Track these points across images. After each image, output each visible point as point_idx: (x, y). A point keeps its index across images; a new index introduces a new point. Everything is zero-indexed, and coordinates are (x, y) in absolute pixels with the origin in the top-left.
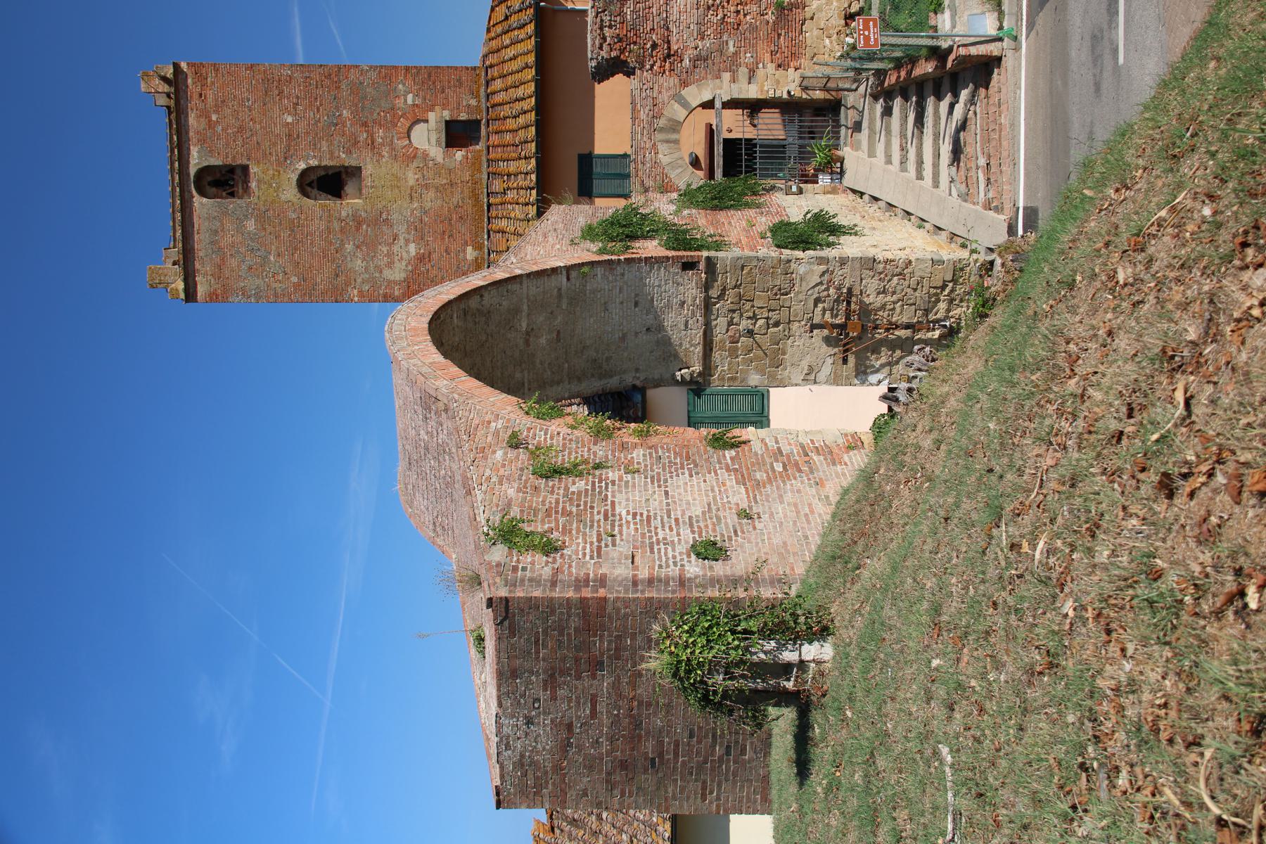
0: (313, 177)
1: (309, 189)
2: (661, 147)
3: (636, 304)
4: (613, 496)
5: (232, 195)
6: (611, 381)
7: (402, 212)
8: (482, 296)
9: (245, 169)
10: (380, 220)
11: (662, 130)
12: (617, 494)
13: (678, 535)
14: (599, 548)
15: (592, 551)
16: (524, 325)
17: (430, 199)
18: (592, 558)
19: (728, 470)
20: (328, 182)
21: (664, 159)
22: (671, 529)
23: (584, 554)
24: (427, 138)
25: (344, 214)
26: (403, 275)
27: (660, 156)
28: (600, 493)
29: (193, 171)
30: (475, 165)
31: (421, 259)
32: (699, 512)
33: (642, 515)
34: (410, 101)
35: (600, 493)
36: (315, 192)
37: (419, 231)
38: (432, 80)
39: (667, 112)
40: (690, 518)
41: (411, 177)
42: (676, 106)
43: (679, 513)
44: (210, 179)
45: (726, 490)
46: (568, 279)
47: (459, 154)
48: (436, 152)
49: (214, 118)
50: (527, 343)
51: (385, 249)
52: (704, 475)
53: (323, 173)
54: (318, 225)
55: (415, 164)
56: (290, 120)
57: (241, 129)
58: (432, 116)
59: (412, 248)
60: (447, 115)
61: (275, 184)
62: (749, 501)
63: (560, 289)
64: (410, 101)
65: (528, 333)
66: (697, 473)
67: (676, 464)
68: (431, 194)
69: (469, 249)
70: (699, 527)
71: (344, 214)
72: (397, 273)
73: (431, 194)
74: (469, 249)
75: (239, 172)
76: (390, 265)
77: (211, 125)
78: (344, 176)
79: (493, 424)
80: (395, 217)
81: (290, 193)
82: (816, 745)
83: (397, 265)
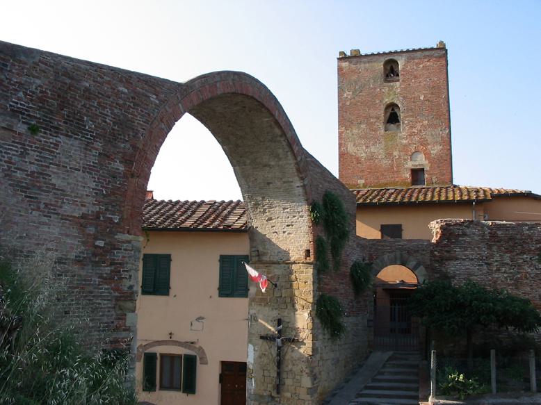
0: (396, 110)
1: (391, 109)
2: (392, 255)
3: (288, 226)
4: (76, 138)
5: (387, 76)
8: (281, 136)
9: (398, 81)
10: (376, 140)
11: (401, 255)
12: (78, 142)
13: (31, 163)
14: (24, 114)
15: (18, 108)
16: (272, 163)
17: (385, 163)
18: (11, 105)
19: (98, 213)
20: (393, 118)
21: (386, 257)
22: (36, 160)
23: (17, 103)
27: (388, 254)
28: (82, 133)
29: (395, 58)
30: (404, 183)
31: (358, 161)
32: (54, 181)
33: (57, 149)
35: (82, 133)
36: (390, 111)
37: (371, 158)
38: (445, 160)
39: (411, 258)
40: (50, 176)
42: (414, 263)
43: (55, 170)
44: (394, 67)
45: (77, 205)
46: (298, 187)
47: (408, 175)
48: (410, 165)
49: (421, 66)
50: (266, 166)
52: (93, 197)
54: (373, 113)
56: (422, 98)
57: (415, 77)
58: (427, 162)
60: (427, 168)
61: (394, 92)
62: (63, 215)
63: (292, 182)
65: (269, 165)
66: (96, 193)
67: (108, 184)
70: (39, 177)
72: (351, 149)
75: (397, 78)
78: (397, 124)
79: (155, 97)
81: (387, 100)
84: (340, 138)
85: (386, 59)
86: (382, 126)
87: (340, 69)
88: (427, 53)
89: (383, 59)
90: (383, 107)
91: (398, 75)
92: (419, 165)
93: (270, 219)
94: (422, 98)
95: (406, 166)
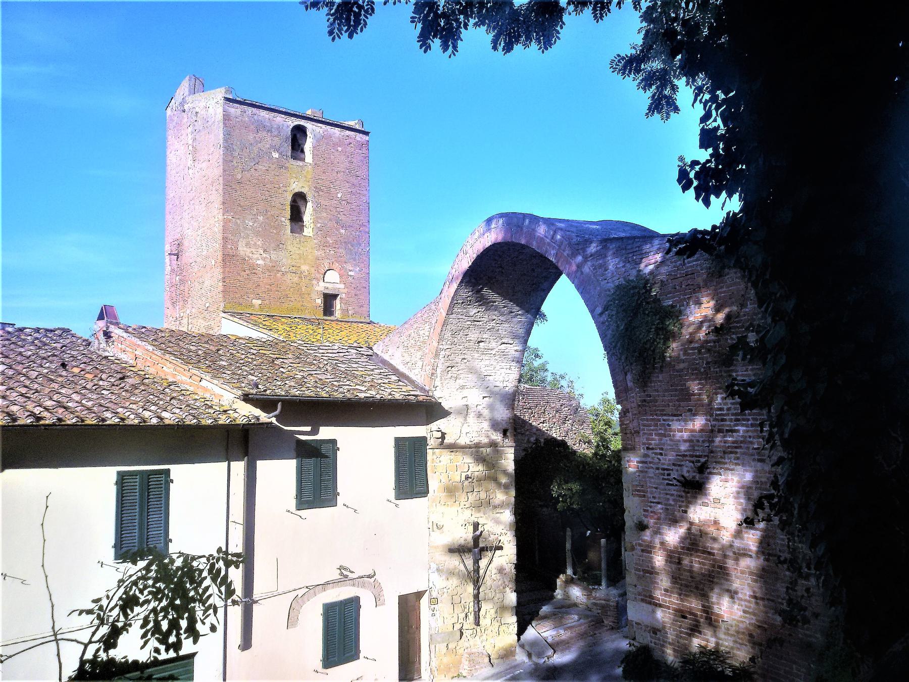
0: (300, 203)
6: (439, 379)
7: (284, 260)
24: (333, 281)
25: (283, 219)
26: (242, 253)
31: (253, 268)
34: (350, 273)
37: (273, 268)
41: (305, 268)
44: (298, 136)
47: (319, 301)
48: (321, 287)
49: (340, 149)
51: (259, 243)
53: (302, 209)
55: (313, 269)
58: (342, 286)
59: (260, 262)
64: (350, 273)
68: (296, 279)
69: (259, 302)
71: (283, 219)
72: (243, 250)
73: (296, 279)
74: (259, 302)
75: (302, 156)
76: (248, 245)
77: (335, 145)
80: (282, 254)
81: (296, 187)
82: (705, 505)
83: (249, 250)
84: (225, 229)
85: (296, 123)
86: (288, 223)
87: (226, 117)
88: (348, 133)
89: (293, 122)
90: (289, 198)
91: (303, 151)
92: (335, 289)
93: (462, 387)
94: (339, 195)
95: (318, 288)
